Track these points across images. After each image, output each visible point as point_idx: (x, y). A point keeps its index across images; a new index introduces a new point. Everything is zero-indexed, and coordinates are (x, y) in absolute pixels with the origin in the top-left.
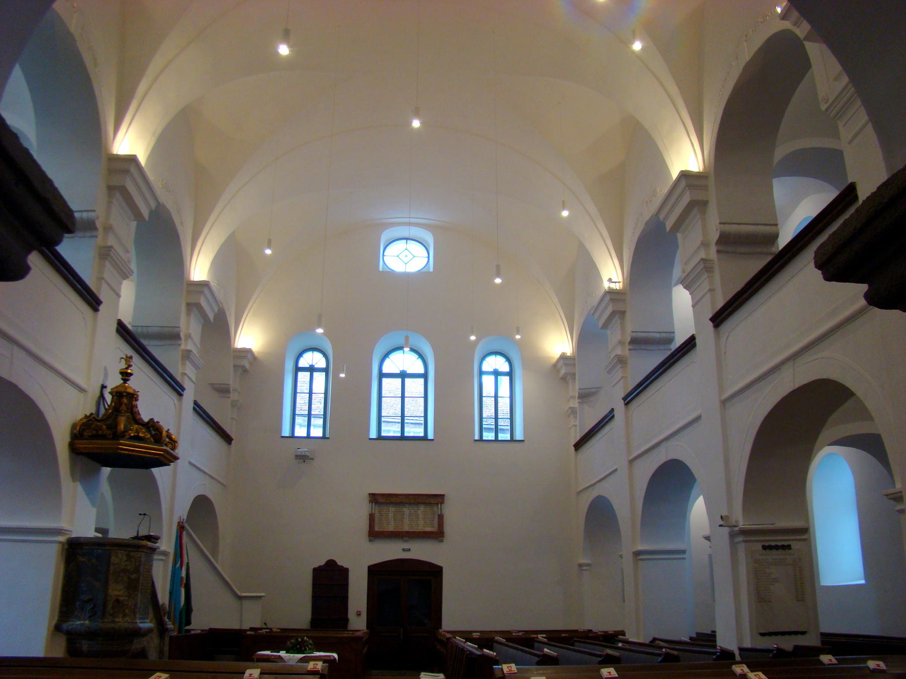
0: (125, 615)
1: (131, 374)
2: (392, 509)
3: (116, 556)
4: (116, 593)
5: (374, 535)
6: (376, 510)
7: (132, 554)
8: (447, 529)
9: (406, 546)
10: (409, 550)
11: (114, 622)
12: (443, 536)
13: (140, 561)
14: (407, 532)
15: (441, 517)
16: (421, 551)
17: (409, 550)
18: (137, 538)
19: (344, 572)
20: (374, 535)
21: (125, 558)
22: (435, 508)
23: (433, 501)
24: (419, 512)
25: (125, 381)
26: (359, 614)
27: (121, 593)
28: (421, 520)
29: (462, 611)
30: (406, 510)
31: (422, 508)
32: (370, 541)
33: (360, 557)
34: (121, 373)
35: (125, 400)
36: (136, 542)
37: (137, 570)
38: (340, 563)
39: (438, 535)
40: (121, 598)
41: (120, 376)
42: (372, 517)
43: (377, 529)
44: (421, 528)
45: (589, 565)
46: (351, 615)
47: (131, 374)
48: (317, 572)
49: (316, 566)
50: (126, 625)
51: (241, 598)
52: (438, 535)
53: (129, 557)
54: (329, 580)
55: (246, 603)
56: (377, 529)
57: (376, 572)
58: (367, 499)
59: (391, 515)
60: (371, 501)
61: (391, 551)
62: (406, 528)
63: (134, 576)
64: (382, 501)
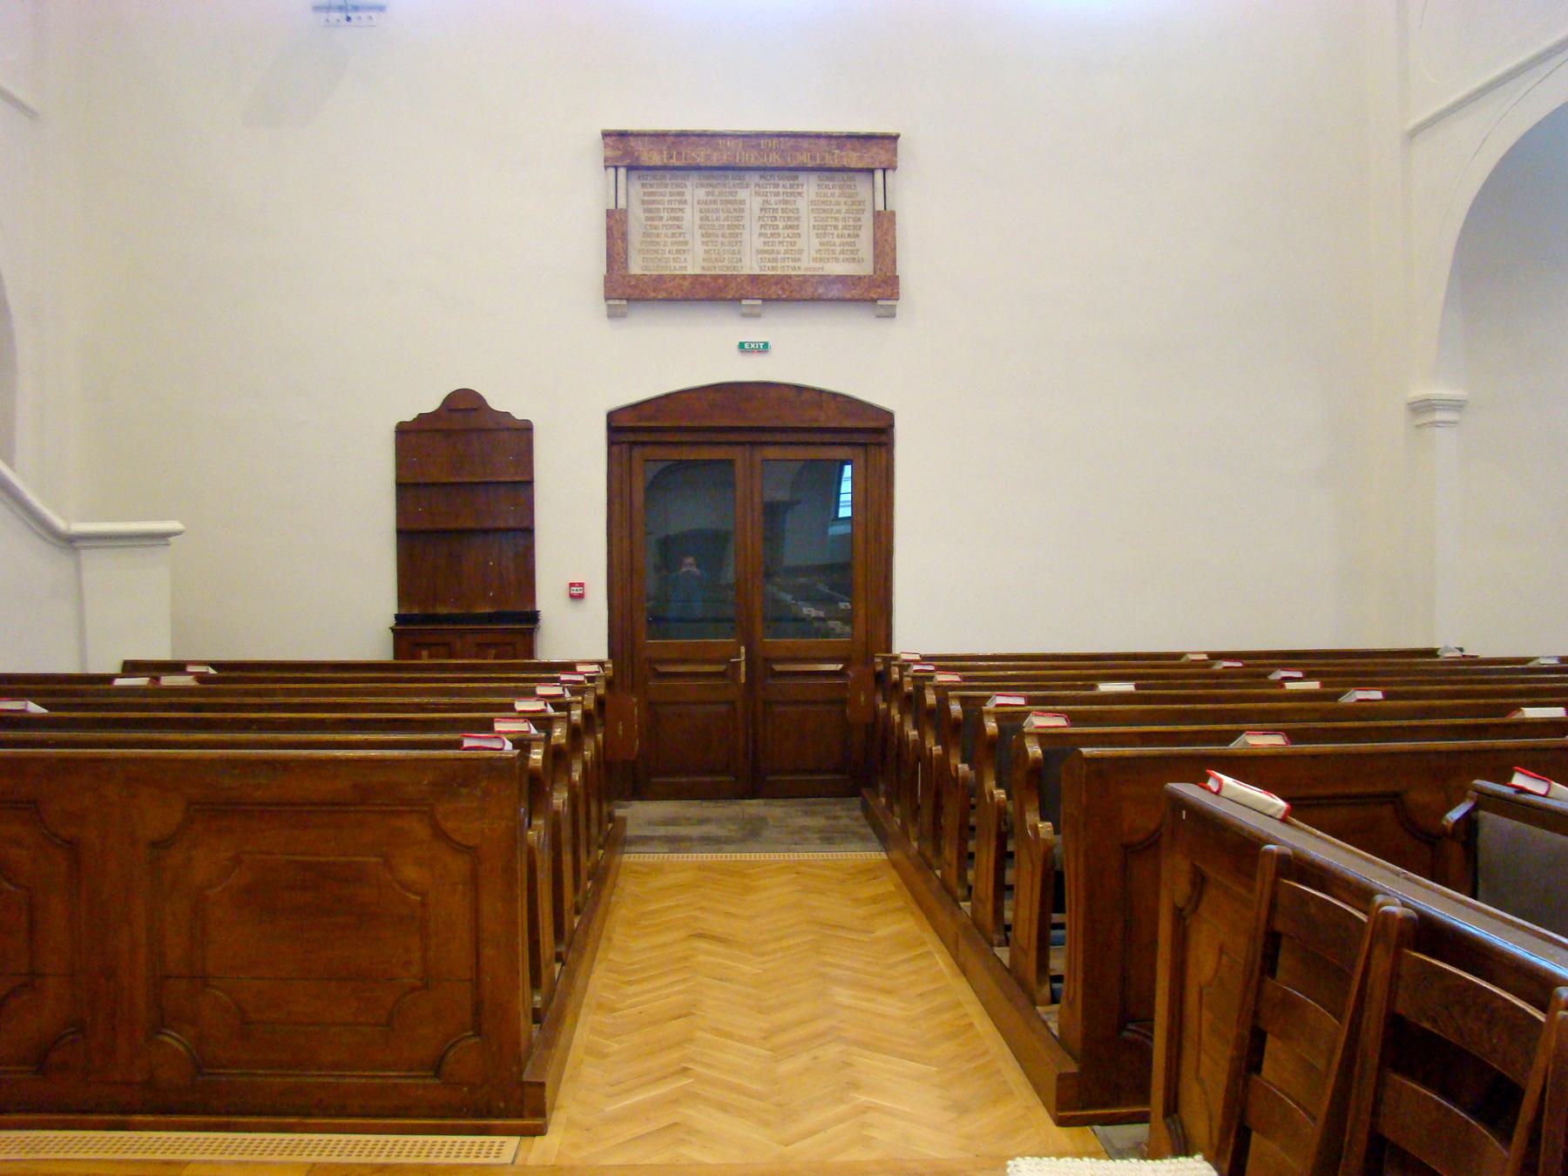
2: (695, 192)
5: (629, 291)
6: (634, 194)
8: (909, 268)
9: (753, 332)
10: (764, 348)
12: (894, 295)
14: (754, 279)
15: (884, 222)
16: (808, 354)
17: (764, 348)
19: (517, 437)
20: (629, 291)
22: (862, 187)
23: (852, 158)
24: (802, 204)
26: (577, 594)
28: (805, 230)
29: (976, 578)
30: (751, 196)
31: (810, 188)
32: (613, 314)
33: (573, 379)
38: (496, 403)
39: (876, 290)
42: (616, 226)
43: (636, 267)
44: (807, 265)
45: (1457, 405)
46: (548, 597)
48: (410, 436)
49: (409, 417)
51: (71, 542)
52: (876, 290)
54: (459, 476)
55: (99, 567)
56: (636, 267)
57: (636, 434)
58: (593, 152)
59: (691, 217)
60: (611, 164)
61: (694, 354)
62: (751, 265)
64: (656, 159)
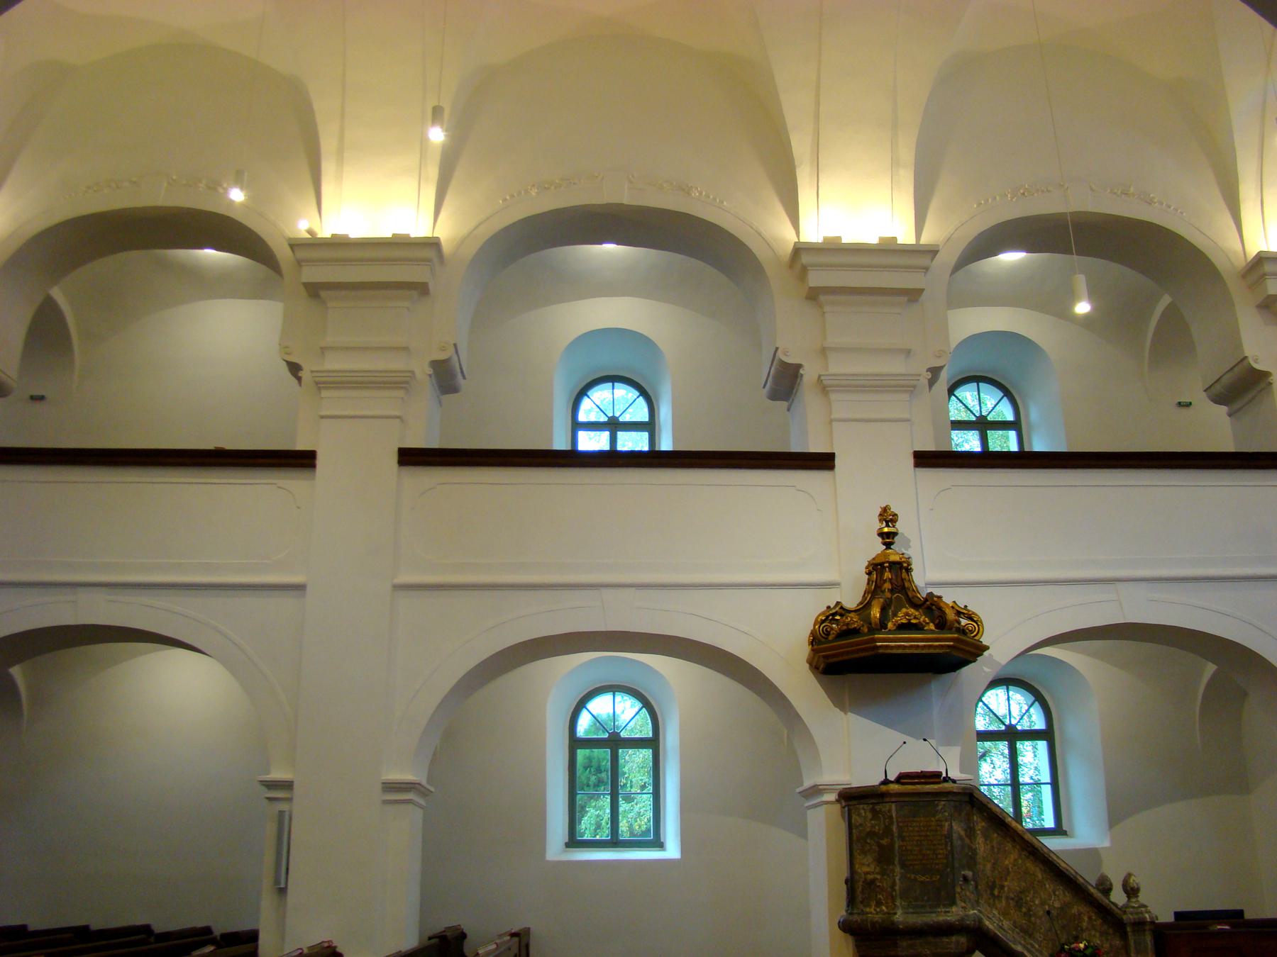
0: (879, 903)
1: (895, 534)
3: (859, 815)
4: (866, 869)
7: (878, 807)
11: (863, 913)
13: (891, 817)
18: (886, 782)
21: (869, 815)
25: (888, 546)
27: (871, 869)
34: (881, 534)
35: (887, 575)
36: (884, 788)
37: (887, 832)
40: (870, 877)
41: (880, 540)
47: (895, 534)
50: (878, 918)
53: (875, 813)
63: (884, 842)
